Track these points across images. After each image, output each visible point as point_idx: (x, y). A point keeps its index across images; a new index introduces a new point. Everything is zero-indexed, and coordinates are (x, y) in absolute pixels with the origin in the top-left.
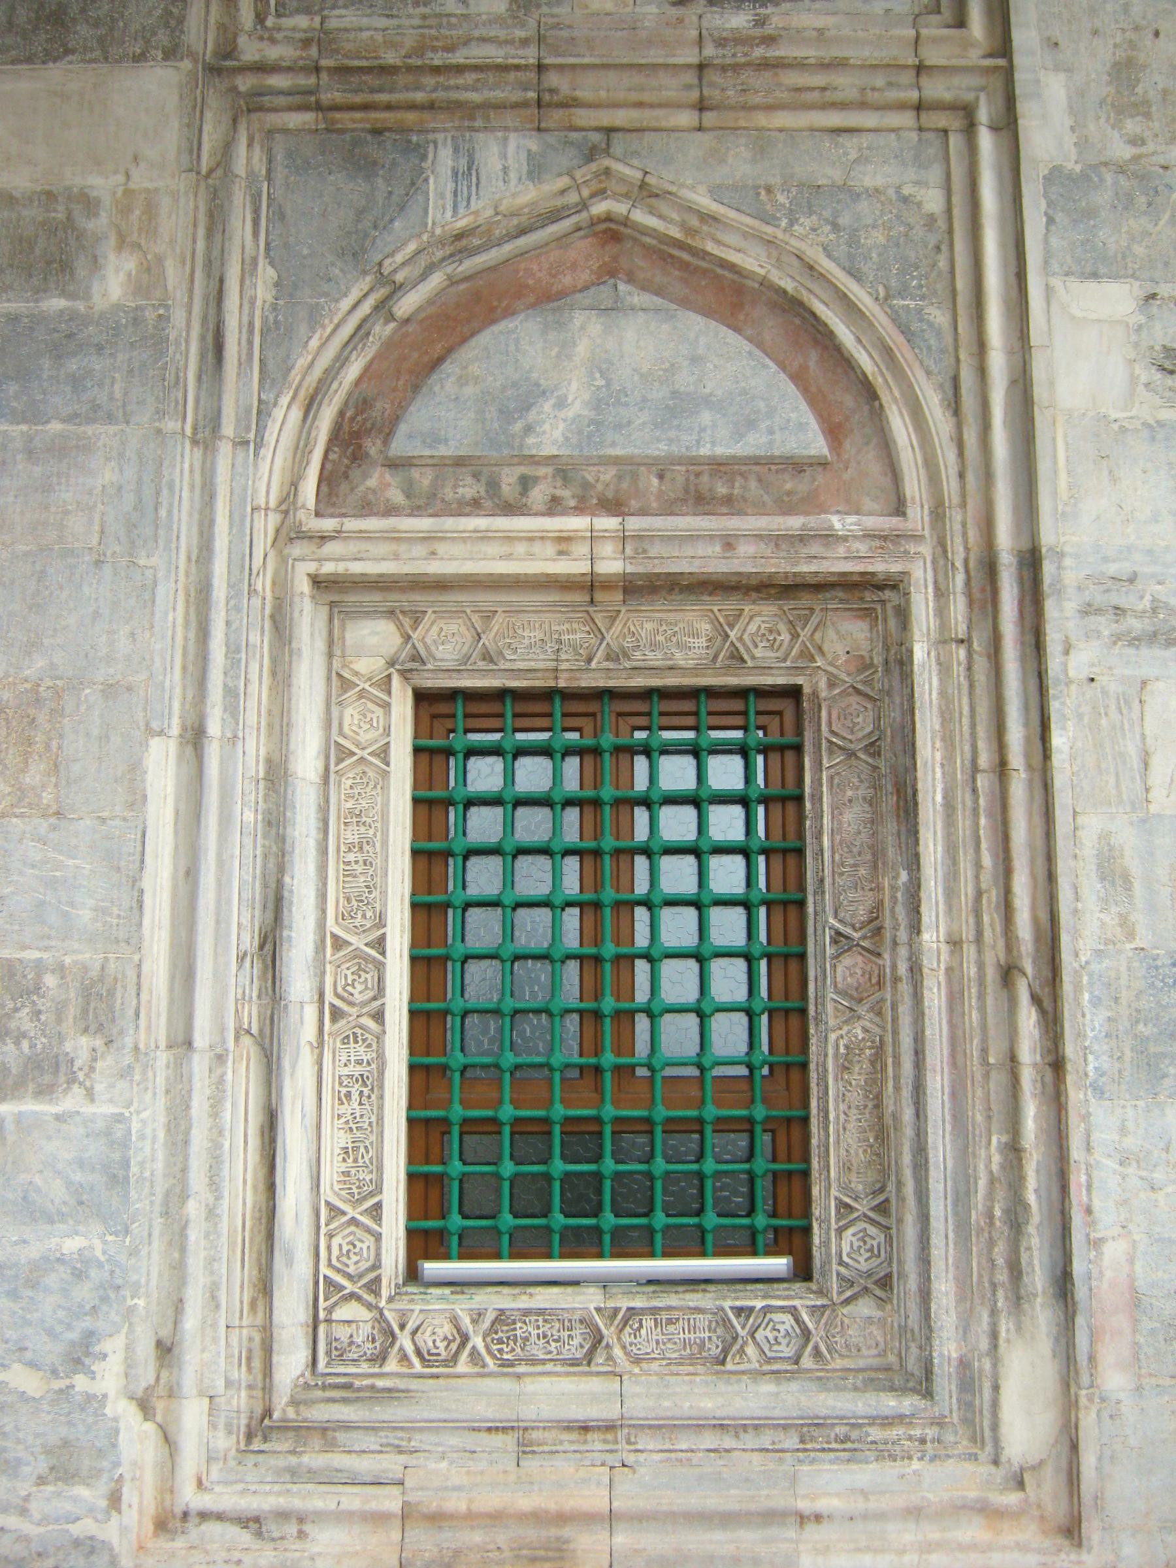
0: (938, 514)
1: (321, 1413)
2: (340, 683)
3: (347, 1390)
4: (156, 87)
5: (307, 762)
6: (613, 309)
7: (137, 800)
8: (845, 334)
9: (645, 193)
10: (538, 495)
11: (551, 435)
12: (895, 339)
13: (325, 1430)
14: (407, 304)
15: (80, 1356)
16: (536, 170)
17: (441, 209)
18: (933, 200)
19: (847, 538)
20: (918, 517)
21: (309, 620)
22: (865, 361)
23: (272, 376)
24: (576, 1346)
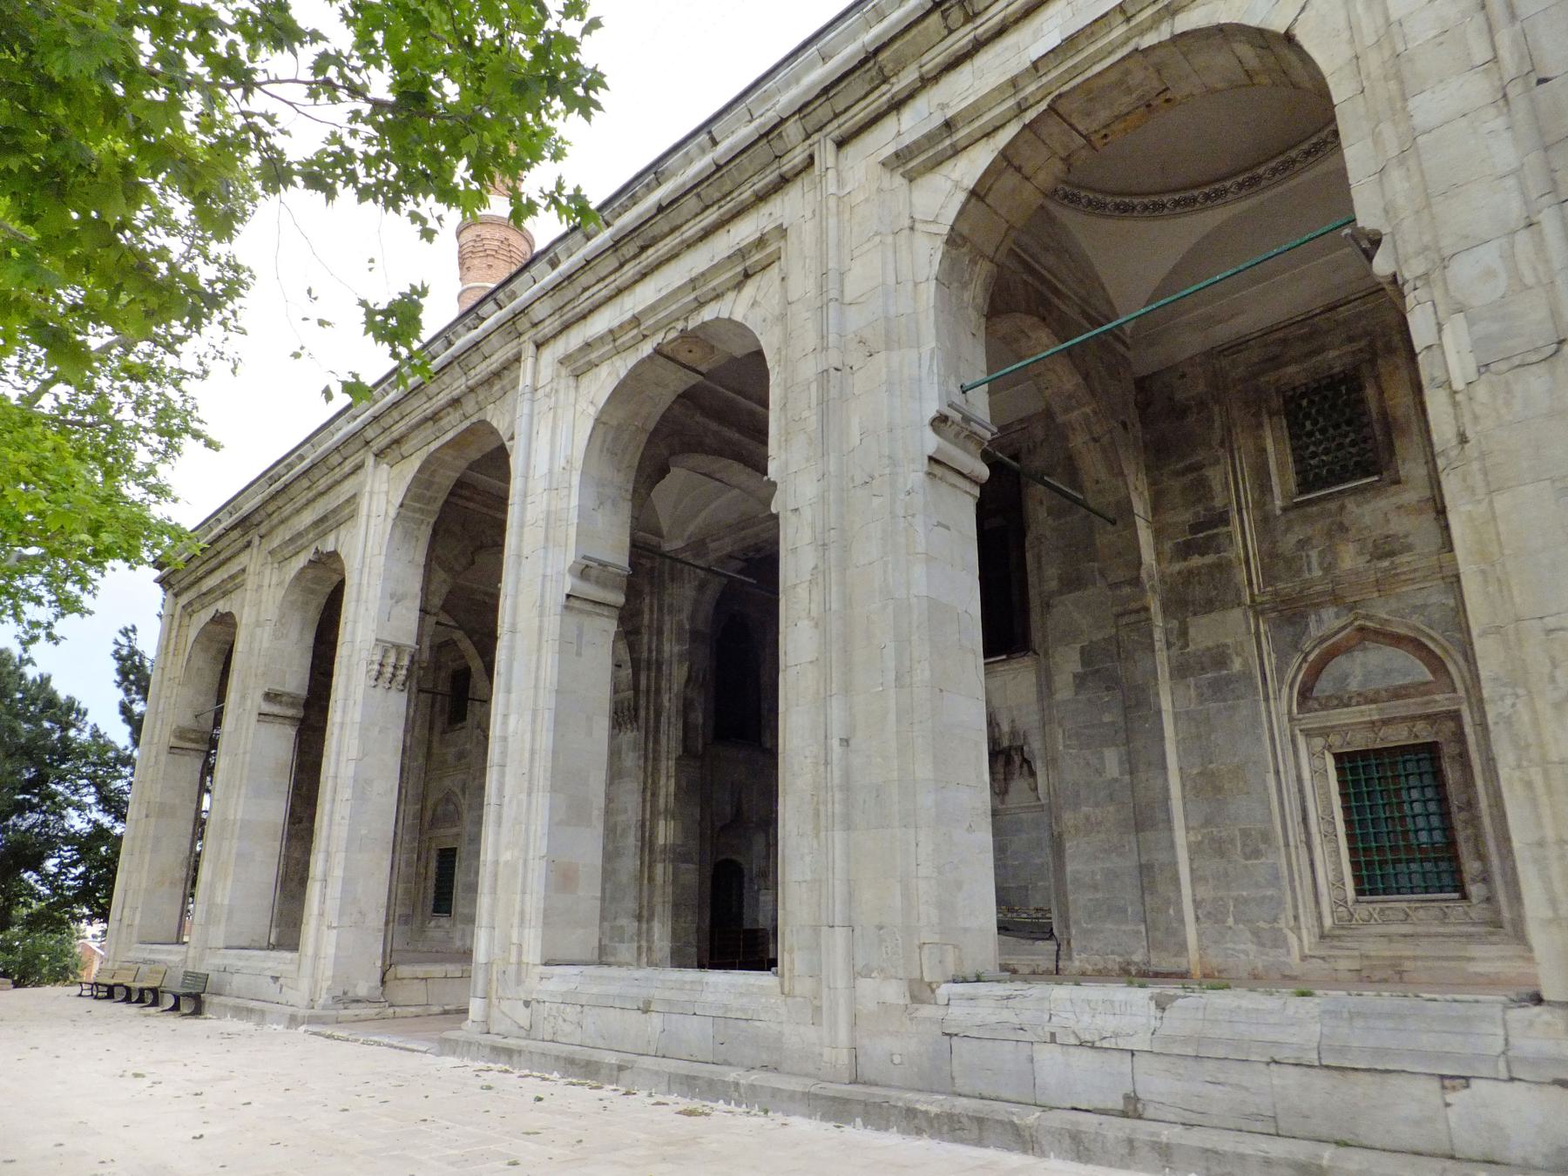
0: (1467, 691)
1: (1337, 932)
2: (1312, 755)
3: (1343, 928)
4: (1236, 614)
5: (1306, 775)
6: (1365, 649)
7: (1266, 789)
8: (1432, 646)
9: (1367, 617)
10: (1354, 702)
11: (1354, 685)
12: (1447, 644)
13: (1338, 937)
14: (1311, 657)
15: (1275, 920)
16: (1337, 616)
17: (1314, 631)
18: (1452, 603)
19: (1441, 701)
20: (1461, 693)
21: (1301, 740)
22: (1438, 651)
23: (1281, 681)
24: (1402, 916)
